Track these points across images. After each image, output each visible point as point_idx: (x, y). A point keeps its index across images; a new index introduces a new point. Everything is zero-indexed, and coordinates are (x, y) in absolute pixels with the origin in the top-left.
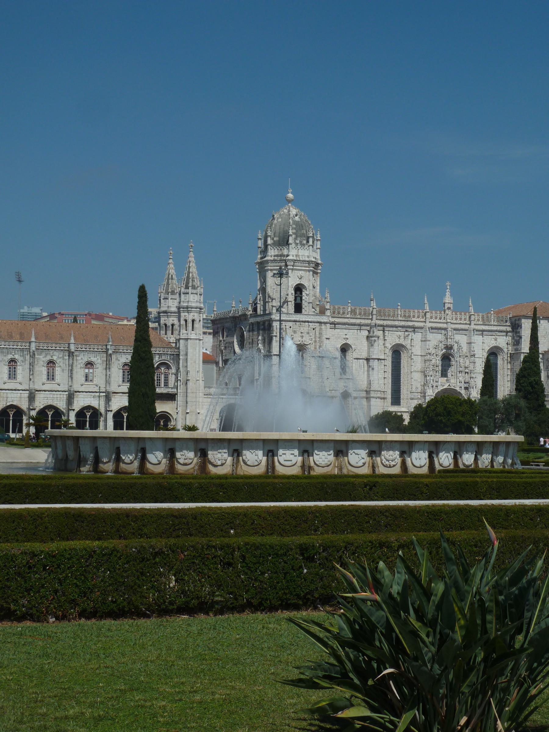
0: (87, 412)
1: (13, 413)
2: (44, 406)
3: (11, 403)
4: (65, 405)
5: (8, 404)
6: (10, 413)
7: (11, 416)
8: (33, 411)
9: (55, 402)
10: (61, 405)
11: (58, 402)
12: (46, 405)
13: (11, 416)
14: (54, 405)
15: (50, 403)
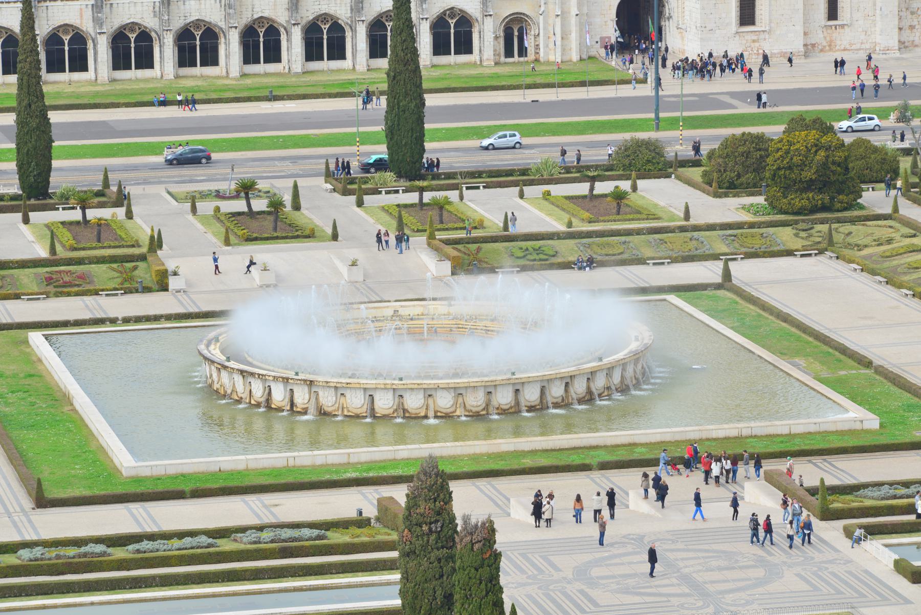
0: (387, 21)
1: (263, 30)
2: (314, 16)
3: (260, 15)
4: (349, 11)
5: (256, 16)
6: (259, 30)
7: (261, 35)
8: (296, 26)
9: (334, 8)
10: (343, 12)
11: (338, 8)
12: (318, 14)
13: (261, 35)
14: (332, 12)
15: (324, 9)
